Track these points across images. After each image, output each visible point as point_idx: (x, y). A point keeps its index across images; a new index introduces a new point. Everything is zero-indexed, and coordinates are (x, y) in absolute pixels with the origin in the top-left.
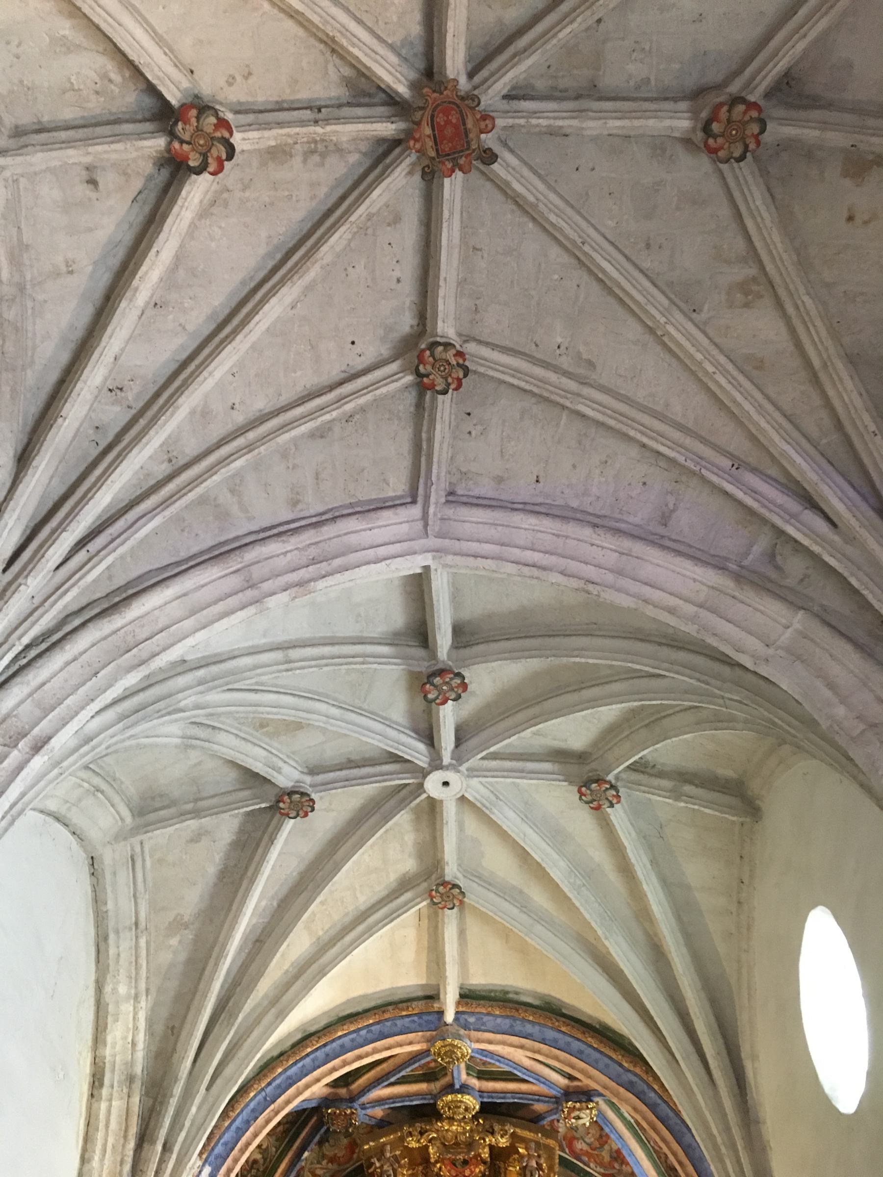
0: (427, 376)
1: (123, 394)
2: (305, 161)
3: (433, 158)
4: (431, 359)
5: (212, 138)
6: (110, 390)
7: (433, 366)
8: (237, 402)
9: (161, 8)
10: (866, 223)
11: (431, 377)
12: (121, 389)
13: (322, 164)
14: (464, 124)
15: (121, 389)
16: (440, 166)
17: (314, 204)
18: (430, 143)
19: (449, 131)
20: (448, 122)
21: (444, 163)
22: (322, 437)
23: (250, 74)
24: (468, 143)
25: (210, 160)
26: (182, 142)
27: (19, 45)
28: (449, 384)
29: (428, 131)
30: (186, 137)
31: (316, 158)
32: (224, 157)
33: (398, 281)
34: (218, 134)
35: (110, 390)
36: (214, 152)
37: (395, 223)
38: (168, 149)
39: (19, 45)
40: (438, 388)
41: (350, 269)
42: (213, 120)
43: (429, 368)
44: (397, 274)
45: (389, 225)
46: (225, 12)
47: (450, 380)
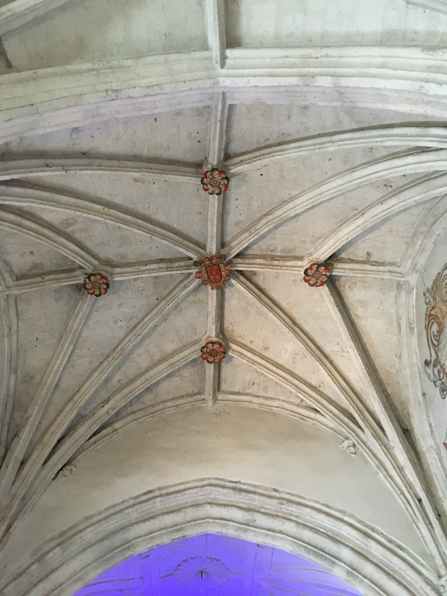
0: (223, 178)
1: (385, 183)
2: (276, 248)
3: (221, 263)
4: (221, 187)
5: (313, 276)
6: (391, 186)
7: (220, 183)
8: (327, 161)
9: (323, 311)
10: (25, 253)
11: (221, 178)
12: (386, 185)
13: (269, 245)
14: (208, 276)
15: (386, 185)
16: (218, 261)
17: (274, 232)
18: (222, 269)
19: (214, 273)
20: (215, 276)
21: (216, 262)
22: (284, 134)
23: (294, 281)
24: (206, 269)
25: (315, 269)
26: (325, 275)
27: (380, 308)
28: (211, 175)
29: (223, 273)
30: (323, 276)
31: (271, 248)
32: (309, 270)
33: (237, 199)
34: (310, 277)
35: (391, 186)
36: (313, 271)
37: (238, 222)
38: (332, 272)
39: (380, 308)
40: (217, 172)
41: (260, 205)
42: (311, 282)
43: (222, 182)
44: (238, 202)
45: (241, 222)
46: (300, 304)
47: (211, 177)
